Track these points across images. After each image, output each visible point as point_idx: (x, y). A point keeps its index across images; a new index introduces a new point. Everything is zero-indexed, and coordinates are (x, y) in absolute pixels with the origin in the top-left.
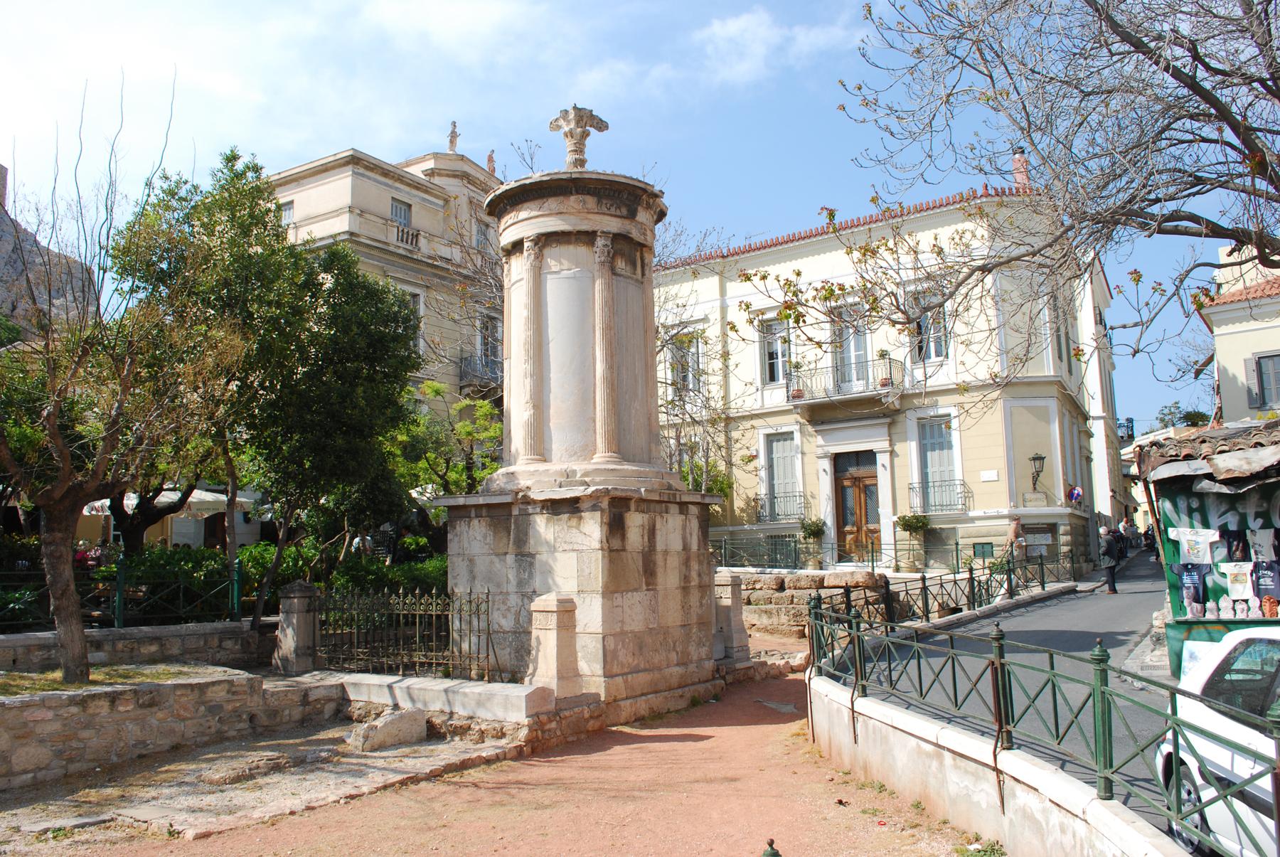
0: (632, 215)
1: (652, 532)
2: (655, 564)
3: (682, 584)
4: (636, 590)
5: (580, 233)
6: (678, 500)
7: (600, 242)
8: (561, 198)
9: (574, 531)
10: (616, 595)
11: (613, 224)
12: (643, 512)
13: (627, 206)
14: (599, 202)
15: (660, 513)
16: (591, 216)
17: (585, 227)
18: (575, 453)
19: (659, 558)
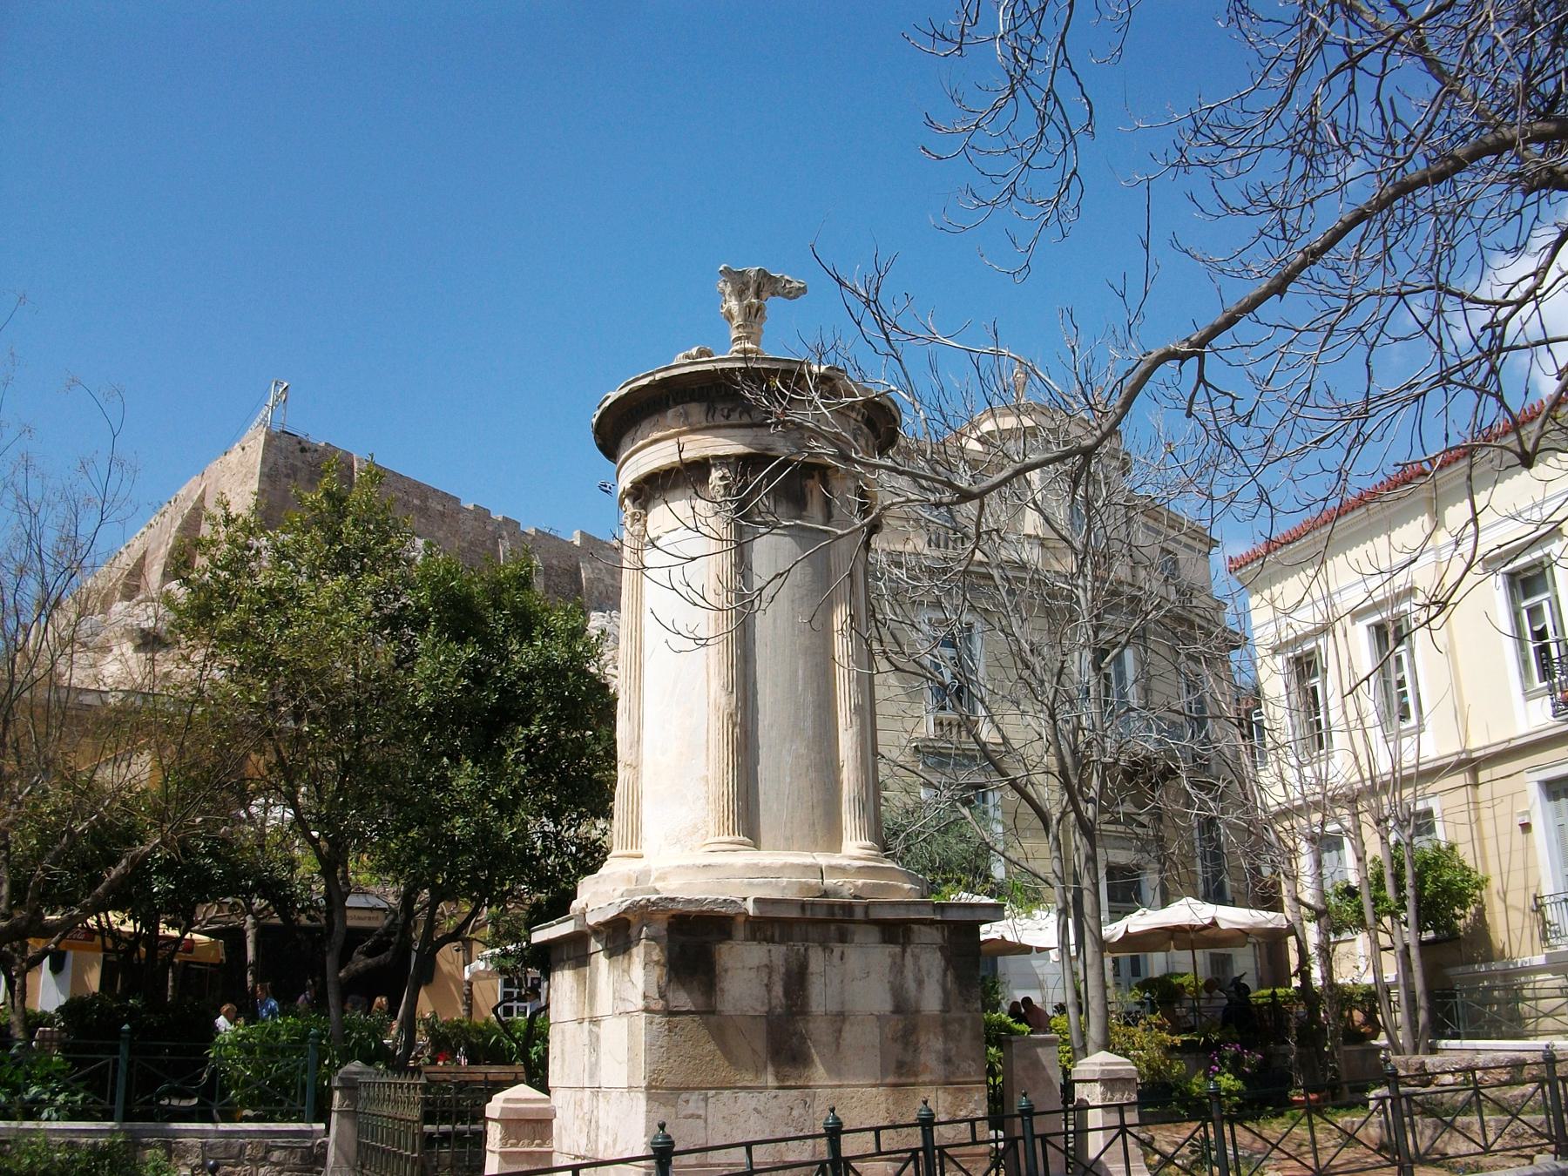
1: (797, 980)
2: (803, 1039)
3: (890, 1079)
7: (715, 475)
8: (656, 417)
10: (684, 1096)
12: (771, 940)
14: (711, 411)
15: (825, 946)
18: (679, 841)
19: (818, 1029)
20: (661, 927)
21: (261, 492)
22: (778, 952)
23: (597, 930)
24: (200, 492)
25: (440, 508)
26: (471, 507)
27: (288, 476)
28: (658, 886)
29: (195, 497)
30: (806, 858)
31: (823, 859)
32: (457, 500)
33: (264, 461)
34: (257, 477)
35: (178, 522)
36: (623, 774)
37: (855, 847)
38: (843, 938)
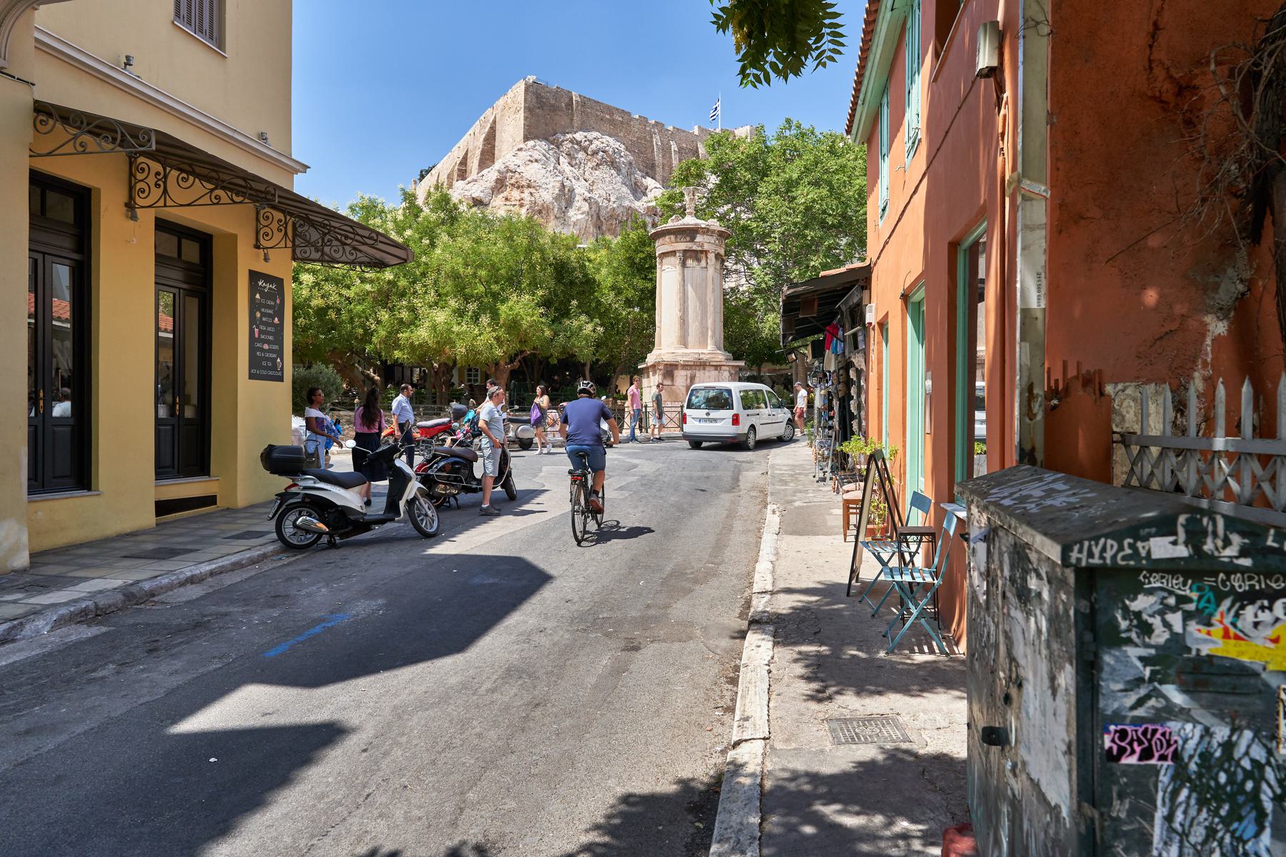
0: (692, 240)
7: (678, 254)
11: (682, 246)
17: (671, 249)
20: (661, 367)
21: (526, 118)
22: (689, 373)
23: (651, 366)
24: (493, 118)
25: (620, 119)
26: (637, 117)
27: (539, 108)
29: (491, 121)
30: (696, 351)
31: (700, 351)
32: (629, 114)
33: (525, 100)
34: (522, 110)
35: (484, 135)
37: (710, 347)
38: (704, 369)
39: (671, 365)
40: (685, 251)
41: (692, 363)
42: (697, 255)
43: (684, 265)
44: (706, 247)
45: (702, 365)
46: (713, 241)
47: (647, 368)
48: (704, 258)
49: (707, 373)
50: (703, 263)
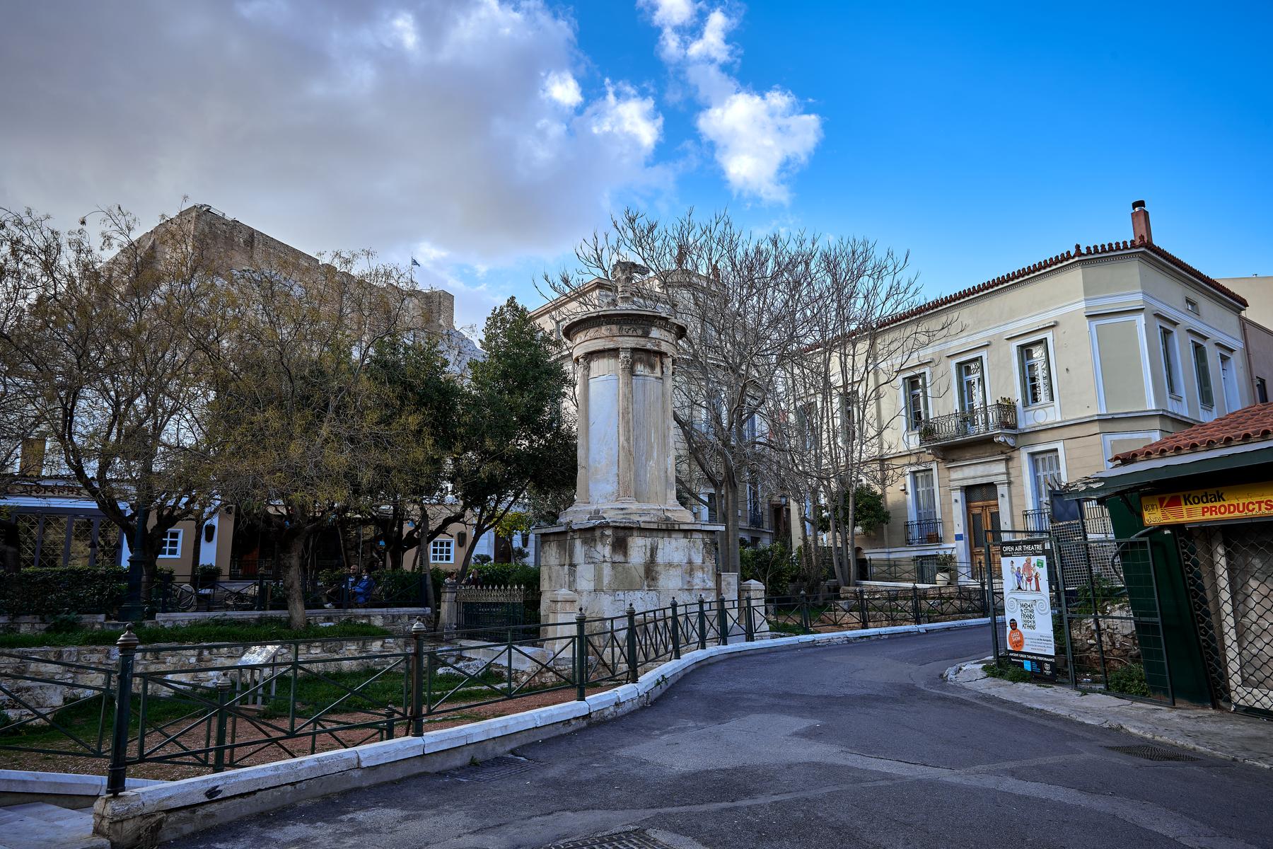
0: (646, 335)
1: (653, 551)
3: (685, 587)
4: (638, 590)
5: (610, 350)
6: (677, 527)
7: (622, 355)
9: (593, 549)
11: (630, 342)
13: (644, 328)
16: (615, 338)
17: (611, 345)
19: (659, 569)
22: (648, 541)
28: (604, 515)
36: (580, 472)
39: (625, 528)
40: (634, 350)
41: (655, 526)
42: (650, 356)
43: (631, 372)
44: (664, 347)
45: (668, 529)
46: (671, 341)
47: (564, 533)
48: (659, 364)
49: (673, 541)
50: (658, 370)
